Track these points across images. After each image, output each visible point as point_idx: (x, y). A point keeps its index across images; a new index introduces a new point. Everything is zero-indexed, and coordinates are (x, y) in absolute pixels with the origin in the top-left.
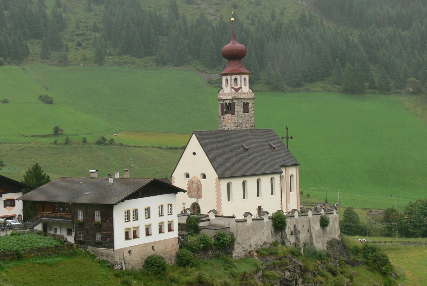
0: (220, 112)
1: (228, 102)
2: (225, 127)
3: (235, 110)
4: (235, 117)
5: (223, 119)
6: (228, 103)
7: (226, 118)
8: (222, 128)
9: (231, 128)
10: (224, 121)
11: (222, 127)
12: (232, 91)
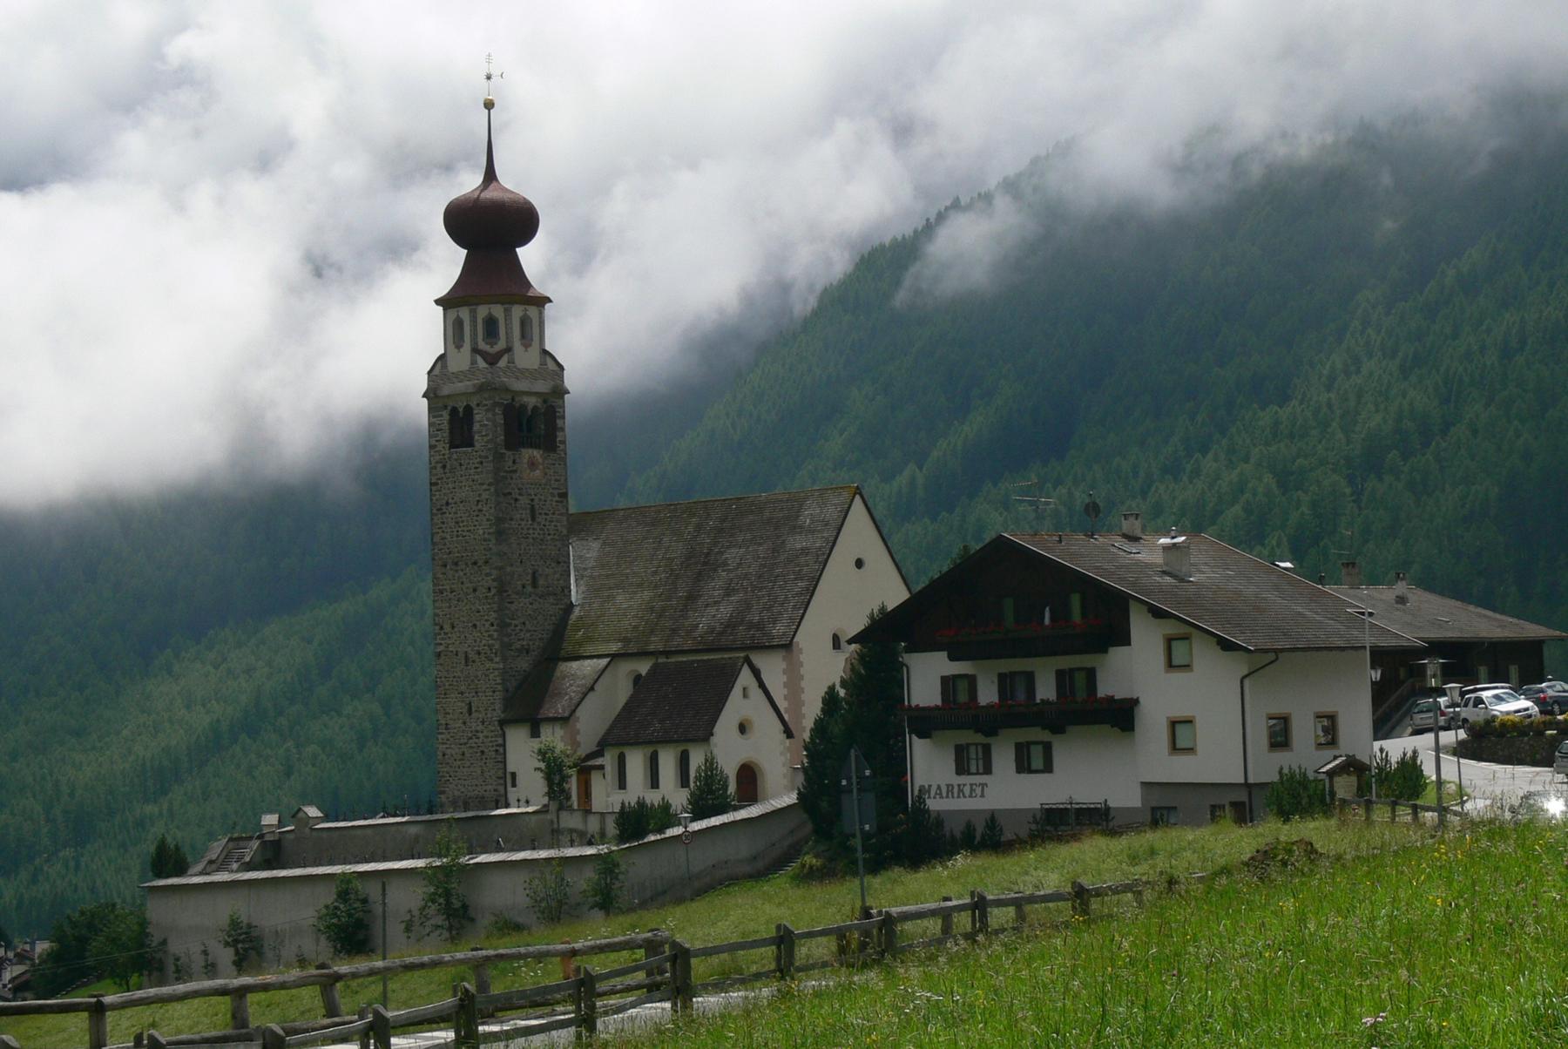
0: (502, 437)
1: (532, 401)
2: (520, 494)
3: (558, 433)
4: (555, 460)
5: (510, 463)
6: (530, 407)
7: (525, 461)
8: (509, 497)
9: (543, 498)
10: (515, 471)
11: (510, 494)
12: (546, 365)
